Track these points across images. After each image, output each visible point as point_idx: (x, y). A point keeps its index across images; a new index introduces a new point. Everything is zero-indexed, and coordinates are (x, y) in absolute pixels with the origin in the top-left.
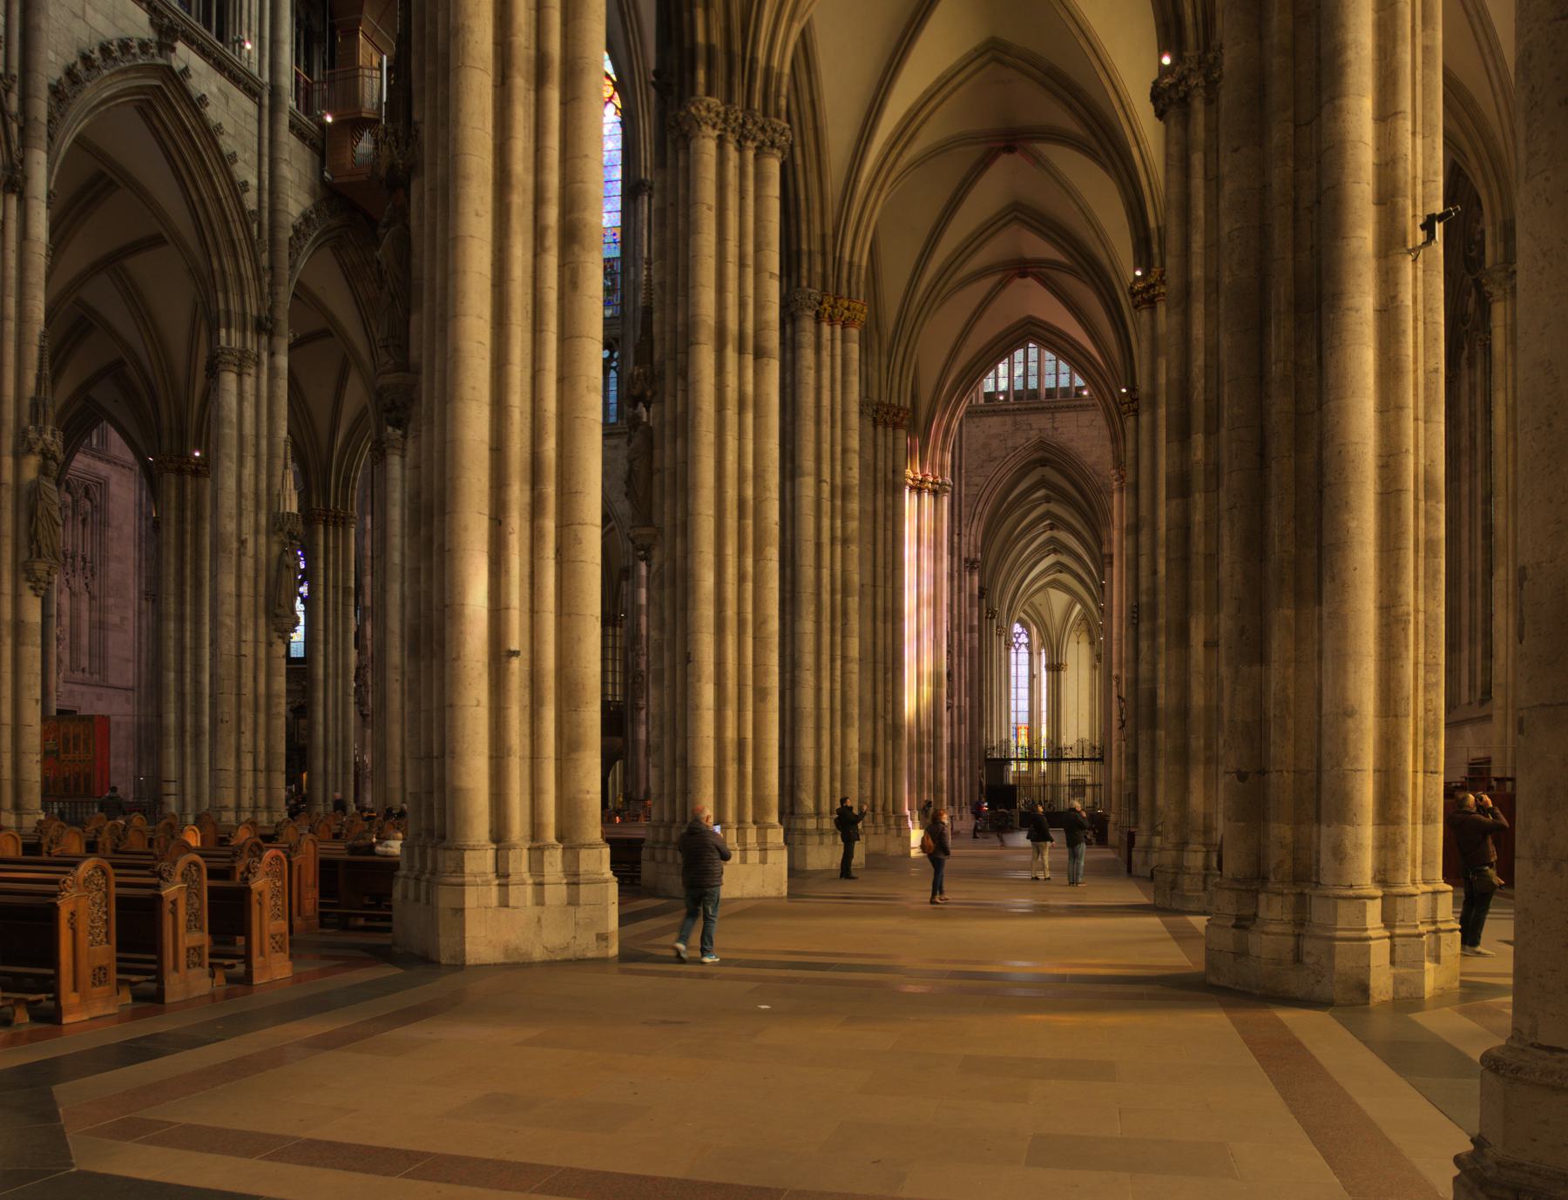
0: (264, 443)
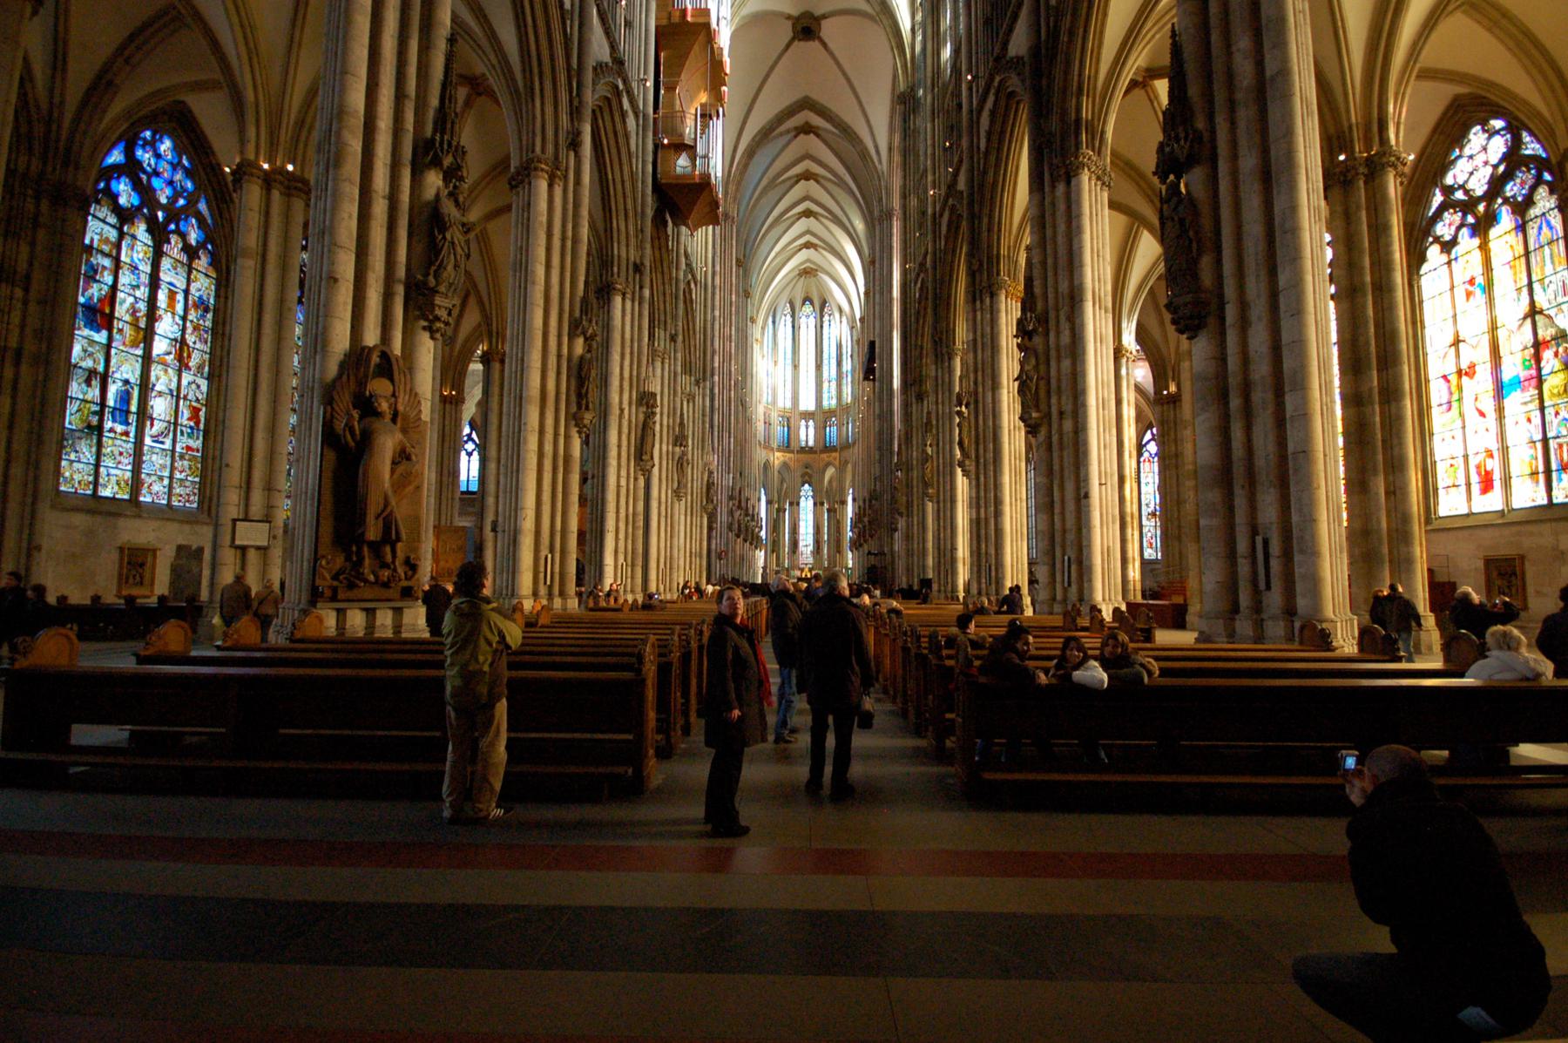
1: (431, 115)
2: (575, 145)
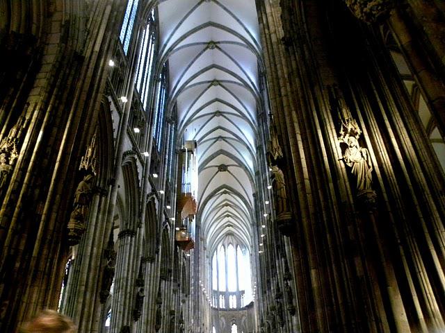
1: (138, 274)
2: (157, 252)
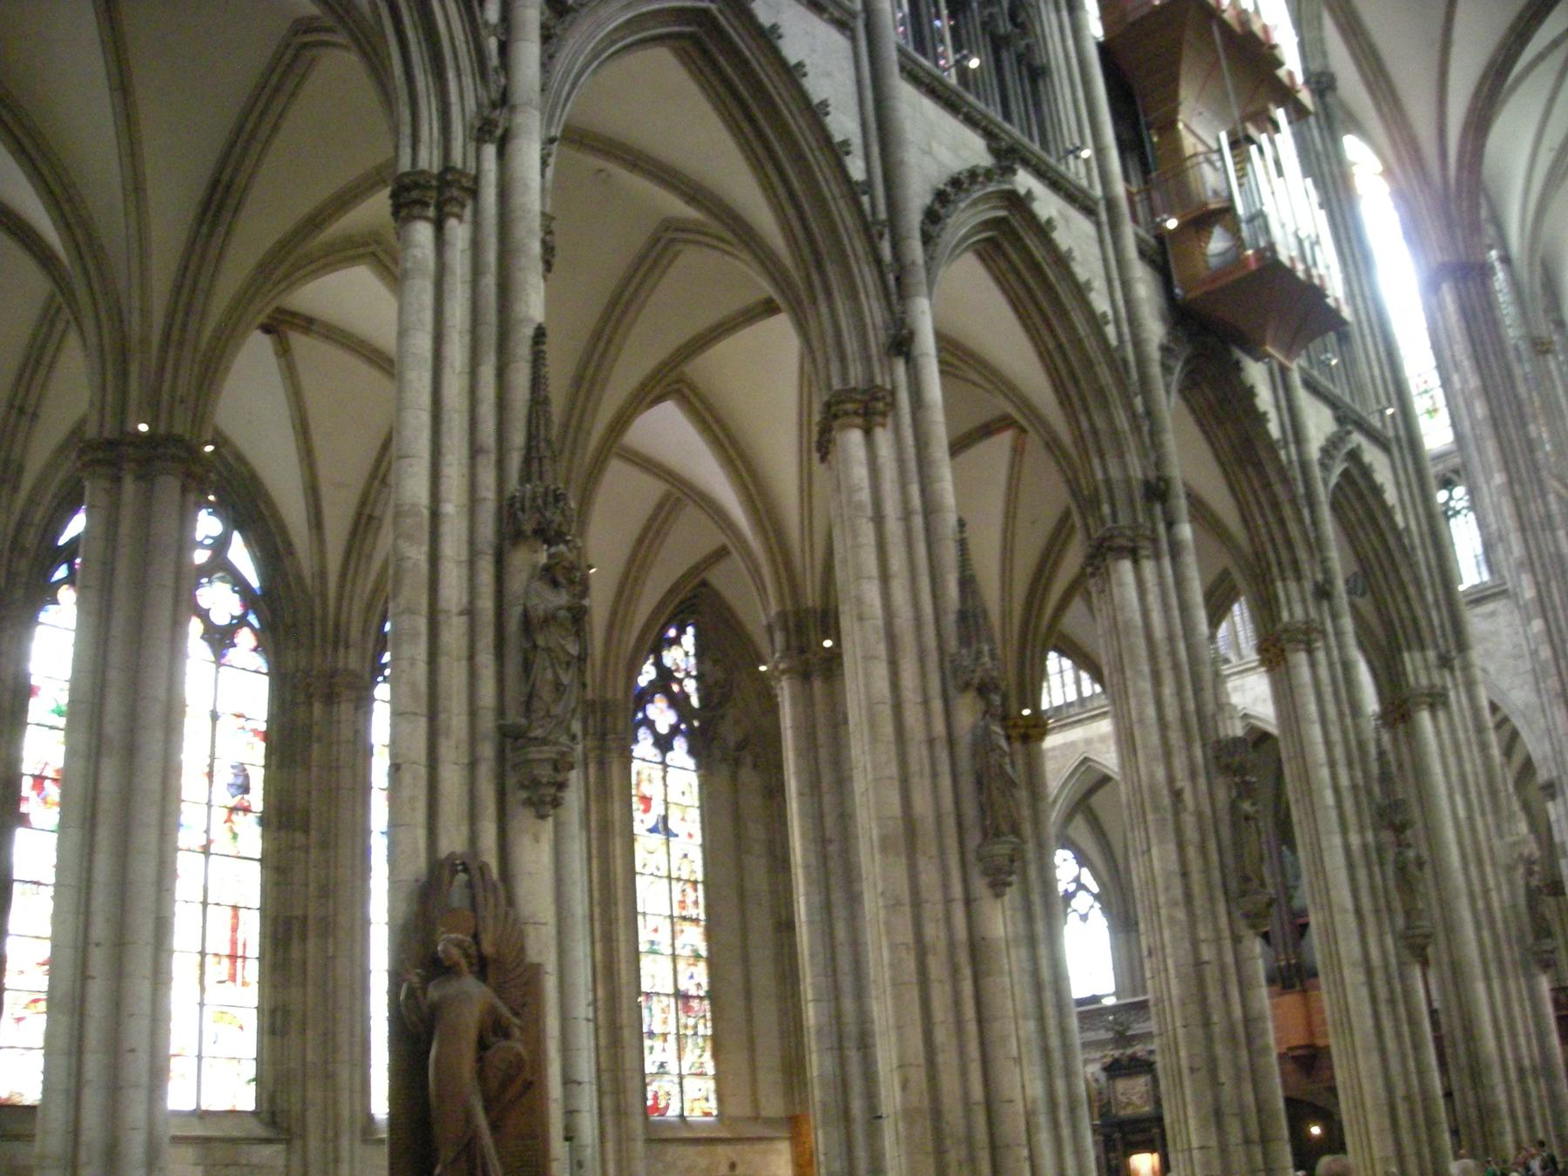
0: (1181, 646)
1: (515, 461)
